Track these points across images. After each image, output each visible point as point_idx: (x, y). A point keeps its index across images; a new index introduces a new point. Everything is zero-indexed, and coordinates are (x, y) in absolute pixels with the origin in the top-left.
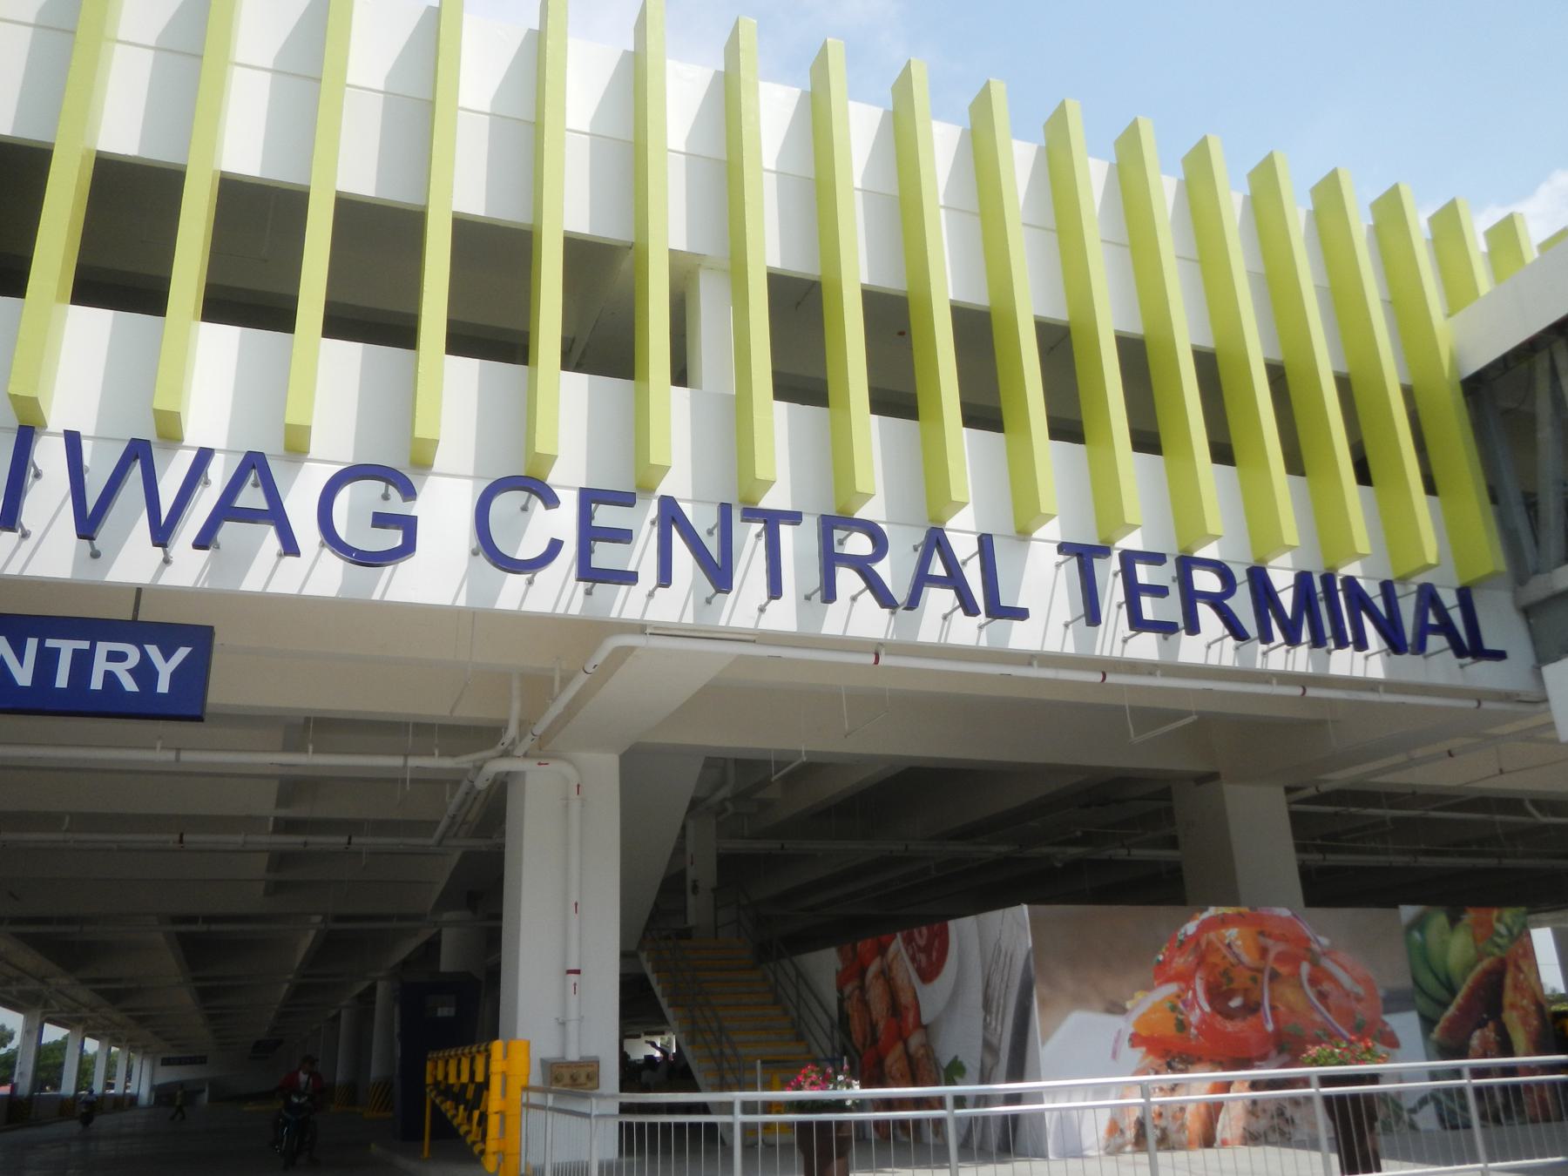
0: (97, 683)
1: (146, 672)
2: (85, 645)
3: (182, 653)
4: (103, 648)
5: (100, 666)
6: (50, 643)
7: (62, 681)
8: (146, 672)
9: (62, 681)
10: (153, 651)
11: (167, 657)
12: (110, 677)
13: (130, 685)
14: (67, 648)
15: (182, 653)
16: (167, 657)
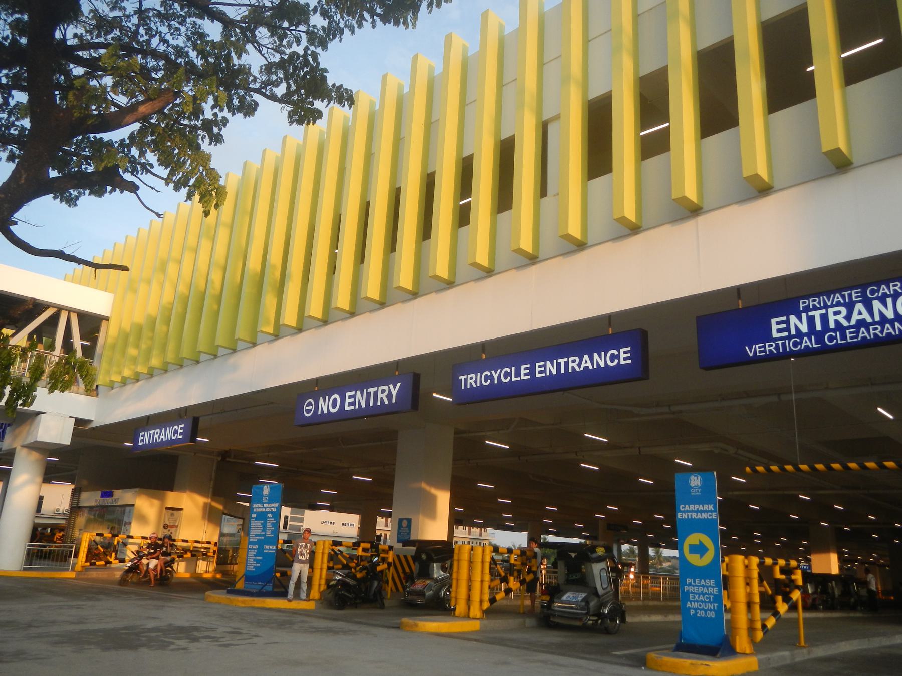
0: (379, 403)
1: (390, 396)
2: (376, 389)
3: (399, 384)
4: (381, 388)
5: (380, 395)
6: (369, 390)
7: (371, 405)
8: (390, 396)
9: (371, 405)
10: (391, 386)
11: (395, 388)
12: (382, 399)
13: (386, 402)
14: (372, 390)
15: (399, 384)
16: (395, 388)
